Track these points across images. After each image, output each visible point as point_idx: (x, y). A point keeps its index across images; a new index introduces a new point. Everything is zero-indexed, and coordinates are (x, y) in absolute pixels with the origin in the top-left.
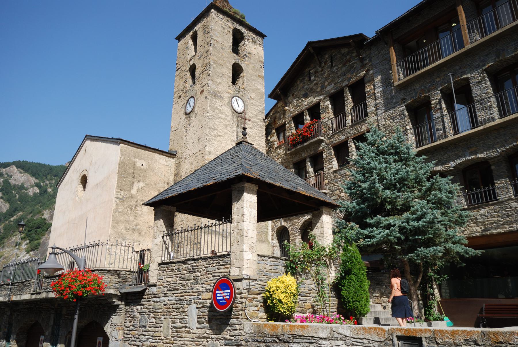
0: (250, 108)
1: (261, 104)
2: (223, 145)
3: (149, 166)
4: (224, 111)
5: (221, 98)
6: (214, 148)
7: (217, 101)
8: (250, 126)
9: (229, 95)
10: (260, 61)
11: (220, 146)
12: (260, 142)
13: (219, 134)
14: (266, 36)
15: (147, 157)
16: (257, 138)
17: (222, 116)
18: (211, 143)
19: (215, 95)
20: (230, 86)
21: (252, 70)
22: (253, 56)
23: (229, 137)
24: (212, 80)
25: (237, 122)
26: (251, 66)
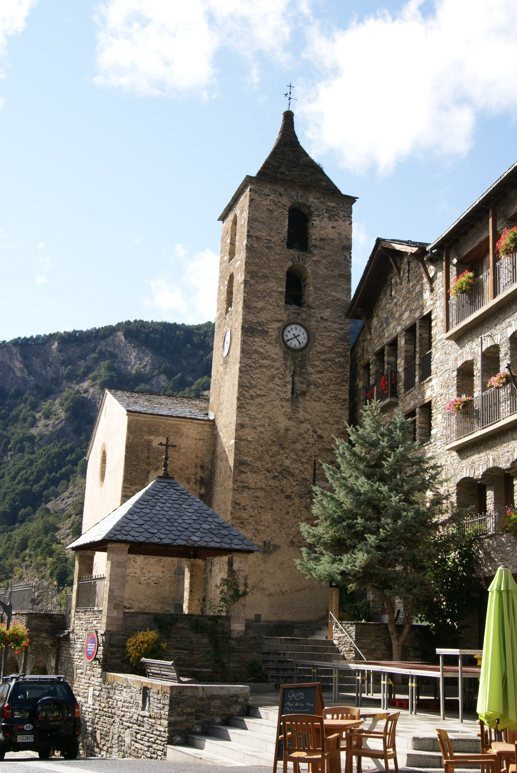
0: (319, 337)
1: (342, 326)
2: (266, 410)
5: (264, 333)
6: (251, 418)
7: (256, 339)
8: (319, 369)
9: (280, 325)
11: (261, 412)
12: (337, 392)
13: (259, 392)
14: (357, 198)
16: (331, 387)
17: (266, 362)
18: (244, 410)
21: (326, 268)
22: (330, 241)
23: (277, 394)
26: (324, 261)
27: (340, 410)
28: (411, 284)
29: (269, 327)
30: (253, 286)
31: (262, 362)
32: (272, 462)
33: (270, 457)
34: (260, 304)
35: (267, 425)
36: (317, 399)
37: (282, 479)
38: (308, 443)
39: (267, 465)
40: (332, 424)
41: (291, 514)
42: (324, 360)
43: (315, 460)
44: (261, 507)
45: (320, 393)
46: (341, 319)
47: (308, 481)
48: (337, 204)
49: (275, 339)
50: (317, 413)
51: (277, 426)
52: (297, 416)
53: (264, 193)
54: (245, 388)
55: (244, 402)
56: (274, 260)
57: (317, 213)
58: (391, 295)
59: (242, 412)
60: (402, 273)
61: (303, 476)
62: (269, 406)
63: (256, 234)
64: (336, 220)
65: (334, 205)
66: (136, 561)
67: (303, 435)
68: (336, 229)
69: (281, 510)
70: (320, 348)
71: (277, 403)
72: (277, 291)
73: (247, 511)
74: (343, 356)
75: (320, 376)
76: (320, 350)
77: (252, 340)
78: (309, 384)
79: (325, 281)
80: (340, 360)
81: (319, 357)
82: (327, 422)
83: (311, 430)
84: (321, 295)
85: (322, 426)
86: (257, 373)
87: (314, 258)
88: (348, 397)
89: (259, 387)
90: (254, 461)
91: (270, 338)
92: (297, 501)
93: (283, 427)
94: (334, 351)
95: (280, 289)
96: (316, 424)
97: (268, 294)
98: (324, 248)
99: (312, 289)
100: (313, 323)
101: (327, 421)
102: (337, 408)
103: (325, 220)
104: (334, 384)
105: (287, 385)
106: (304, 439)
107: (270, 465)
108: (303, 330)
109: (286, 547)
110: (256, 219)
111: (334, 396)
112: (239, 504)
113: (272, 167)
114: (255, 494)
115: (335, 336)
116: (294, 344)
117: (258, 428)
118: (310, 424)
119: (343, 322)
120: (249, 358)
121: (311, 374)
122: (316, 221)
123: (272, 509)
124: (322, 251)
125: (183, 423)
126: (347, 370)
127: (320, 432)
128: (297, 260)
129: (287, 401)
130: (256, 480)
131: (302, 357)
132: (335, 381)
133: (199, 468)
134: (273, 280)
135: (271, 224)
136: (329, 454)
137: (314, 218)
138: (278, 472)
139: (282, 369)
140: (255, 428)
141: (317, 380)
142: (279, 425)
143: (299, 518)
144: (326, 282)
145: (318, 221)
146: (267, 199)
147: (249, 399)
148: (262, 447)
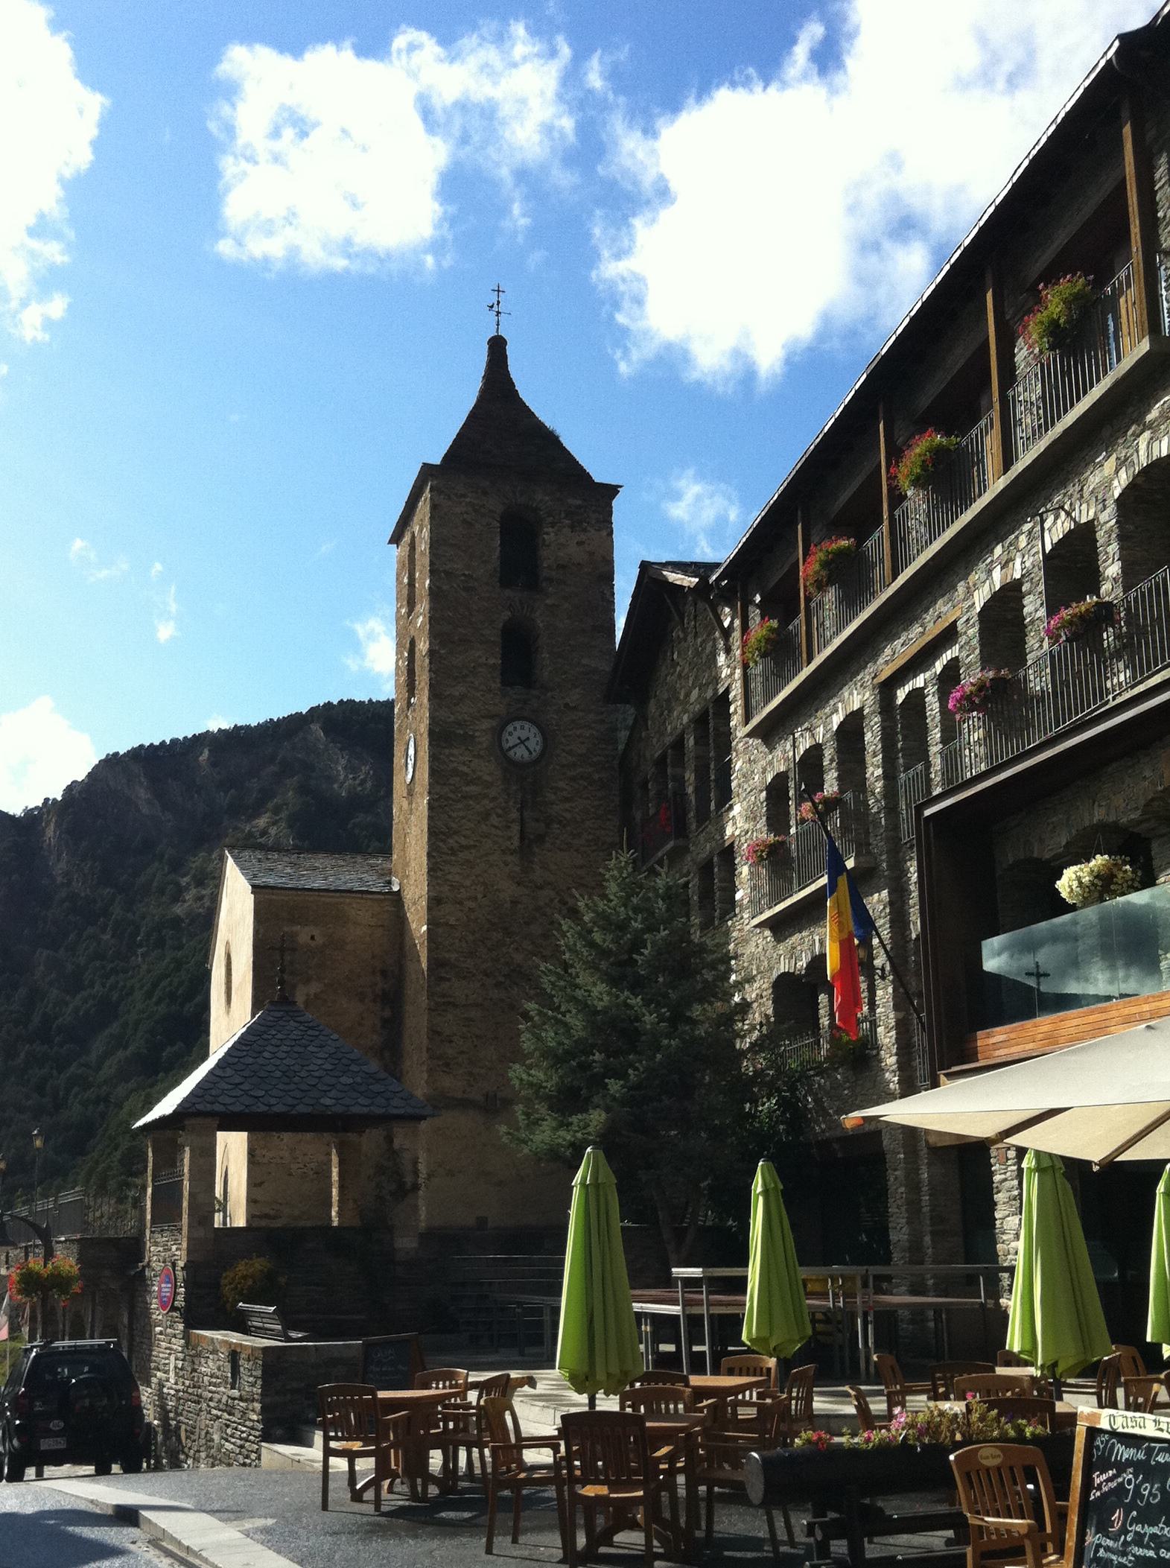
7: (455, 752)
8: (565, 793)
9: (494, 723)
13: (463, 842)
14: (621, 487)
17: (472, 789)
18: (439, 874)
29: (477, 728)
31: (468, 789)
33: (489, 950)
34: (458, 690)
35: (480, 896)
42: (573, 779)
44: (477, 1036)
49: (486, 748)
59: (437, 878)
64: (585, 530)
65: (579, 502)
72: (485, 664)
75: (567, 806)
82: (583, 885)
83: (556, 901)
86: (460, 809)
87: (548, 602)
95: (492, 661)
106: (545, 915)
108: (534, 730)
112: (439, 1034)
116: (520, 753)
118: (553, 890)
119: (603, 709)
120: (445, 784)
121: (552, 804)
122: (549, 535)
125: (348, 900)
138: (504, 976)
140: (461, 903)
141: (564, 814)
144: (572, 642)
145: (553, 534)
146: (461, 503)
148: (473, 934)
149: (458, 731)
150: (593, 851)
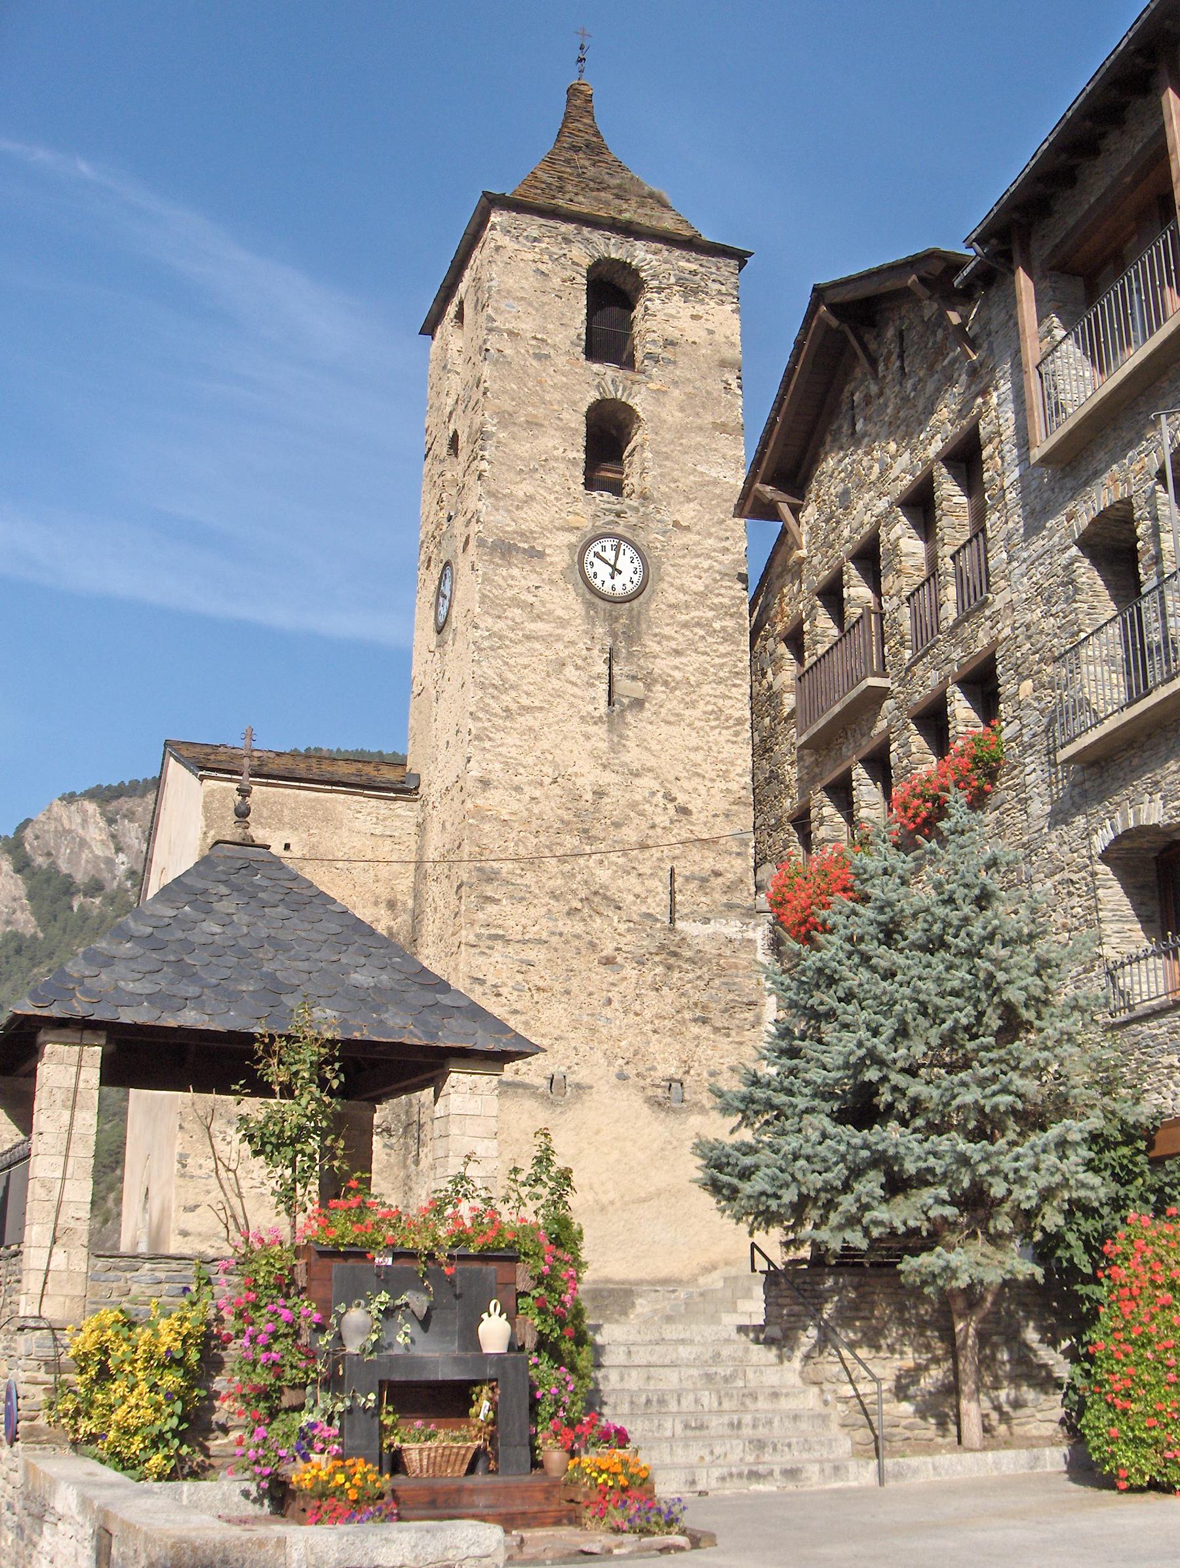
1: (727, 544)
3: (313, 848)
4: (552, 607)
5: (536, 554)
6: (507, 764)
7: (515, 572)
8: (673, 644)
9: (573, 538)
10: (723, 364)
12: (720, 702)
13: (525, 701)
14: (750, 254)
15: (305, 816)
16: (706, 689)
17: (540, 627)
18: (487, 744)
19: (504, 550)
20: (576, 500)
21: (682, 409)
23: (572, 705)
24: (491, 494)
25: (609, 641)
27: (730, 745)
28: (909, 384)
29: (548, 542)
30: (505, 445)
31: (533, 626)
32: (563, 874)
35: (547, 780)
36: (672, 719)
37: (590, 916)
38: (653, 827)
39: (551, 882)
40: (713, 780)
41: (615, 1004)
42: (685, 625)
43: (672, 870)
44: (538, 989)
45: (679, 702)
46: (723, 526)
47: (657, 920)
48: (701, 265)
50: (673, 752)
51: (575, 784)
52: (623, 759)
53: (525, 234)
54: (491, 690)
55: (487, 724)
56: (554, 386)
57: (655, 283)
58: (854, 433)
60: (881, 367)
61: (644, 909)
62: (553, 735)
63: (508, 326)
64: (702, 301)
65: (693, 267)
66: (229, 1139)
67: (641, 807)
68: (703, 320)
69: (591, 994)
70: (673, 596)
71: (572, 728)
73: (503, 1000)
74: (732, 616)
75: (677, 661)
76: (674, 601)
77: (504, 573)
78: (649, 681)
79: (681, 438)
80: (725, 623)
81: (672, 617)
82: (698, 775)
83: (660, 795)
84: (673, 470)
85: (685, 784)
86: (521, 654)
88: (748, 714)
89: (525, 688)
90: (518, 872)
91: (550, 569)
92: (630, 972)
93: (588, 788)
94: (709, 602)
95: (572, 454)
96: (672, 778)
97: (542, 466)
98: (675, 362)
99: (650, 455)
100: (652, 537)
101: (700, 771)
102: (722, 739)
103: (676, 298)
104: (714, 681)
105: (597, 683)
106: (644, 815)
107: (559, 882)
109: (606, 1088)
110: (509, 292)
111: (713, 711)
113: (544, 186)
114: (523, 956)
115: (711, 568)
117: (526, 789)
120: (499, 617)
121: (655, 657)
123: (568, 992)
124: (671, 367)
126: (742, 648)
127: (682, 798)
128: (612, 388)
129: (598, 721)
130: (523, 921)
131: (631, 618)
132: (715, 674)
133: (383, 905)
134: (553, 432)
135: (544, 304)
136: (706, 853)
137: (649, 295)
138: (581, 900)
139: (581, 645)
140: (518, 789)
141: (672, 673)
142: (580, 781)
143: (637, 1014)
144: (683, 441)
145: (658, 302)
147: (501, 718)
149: (521, 545)
150: (712, 728)
